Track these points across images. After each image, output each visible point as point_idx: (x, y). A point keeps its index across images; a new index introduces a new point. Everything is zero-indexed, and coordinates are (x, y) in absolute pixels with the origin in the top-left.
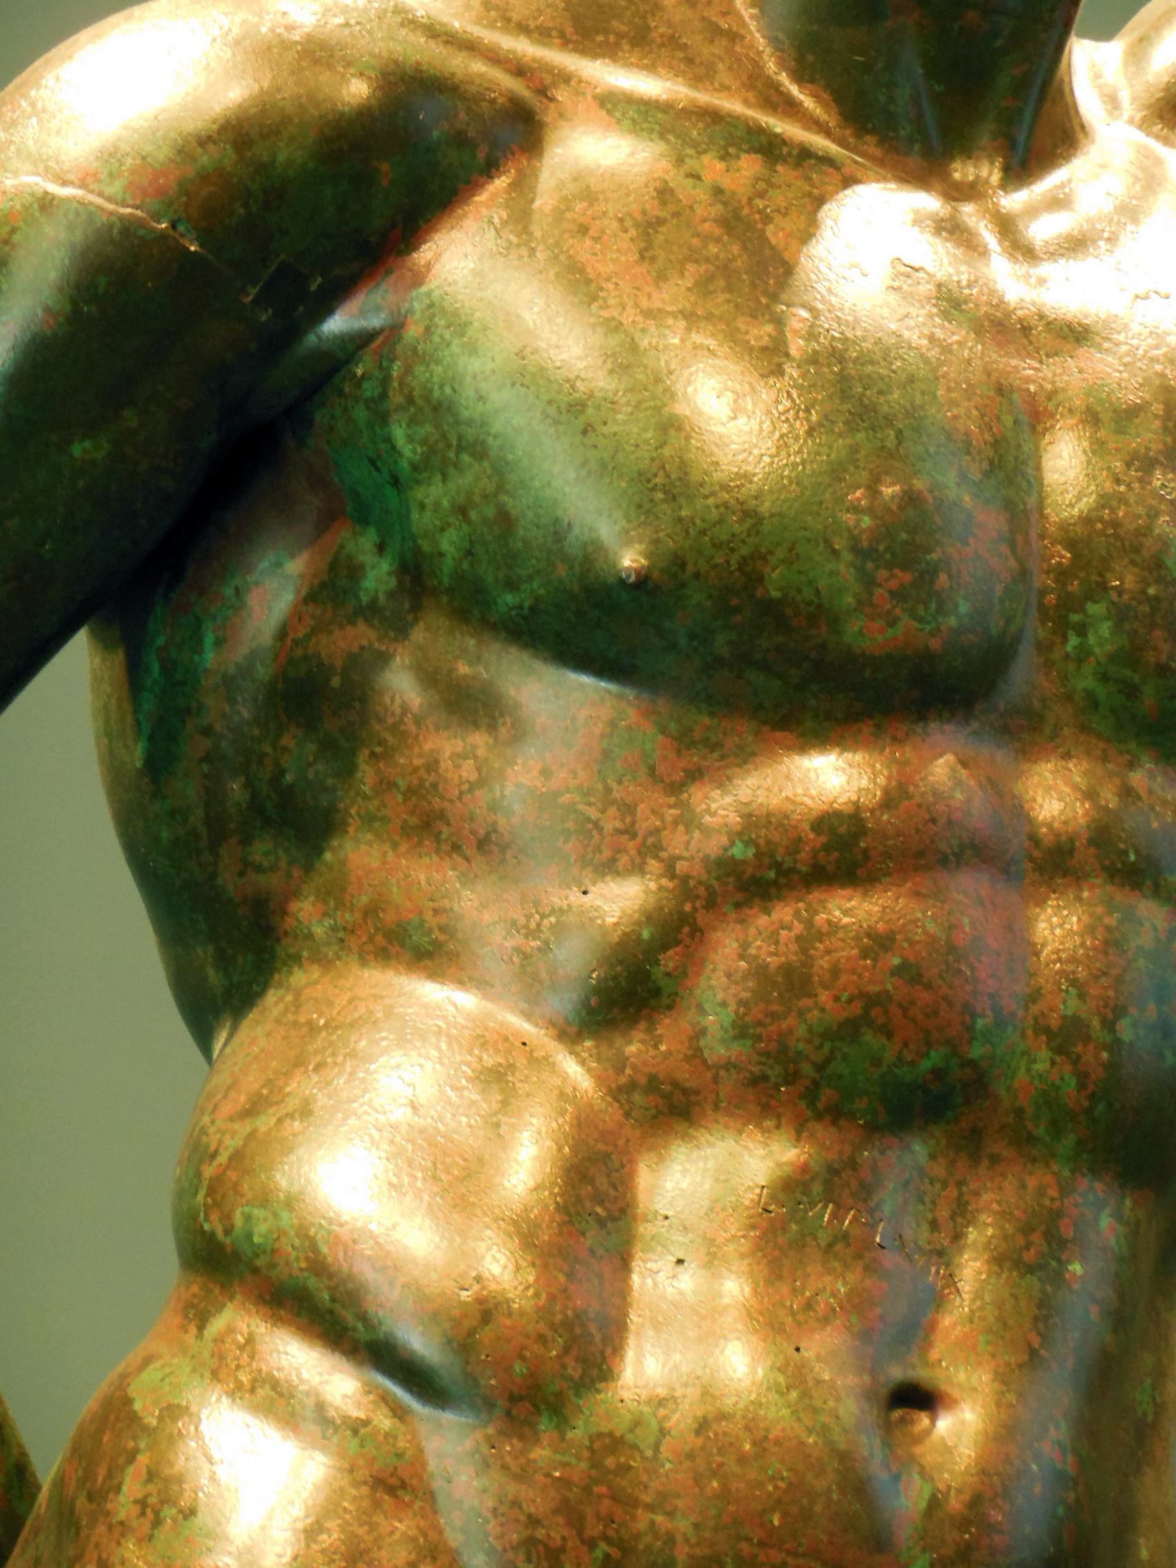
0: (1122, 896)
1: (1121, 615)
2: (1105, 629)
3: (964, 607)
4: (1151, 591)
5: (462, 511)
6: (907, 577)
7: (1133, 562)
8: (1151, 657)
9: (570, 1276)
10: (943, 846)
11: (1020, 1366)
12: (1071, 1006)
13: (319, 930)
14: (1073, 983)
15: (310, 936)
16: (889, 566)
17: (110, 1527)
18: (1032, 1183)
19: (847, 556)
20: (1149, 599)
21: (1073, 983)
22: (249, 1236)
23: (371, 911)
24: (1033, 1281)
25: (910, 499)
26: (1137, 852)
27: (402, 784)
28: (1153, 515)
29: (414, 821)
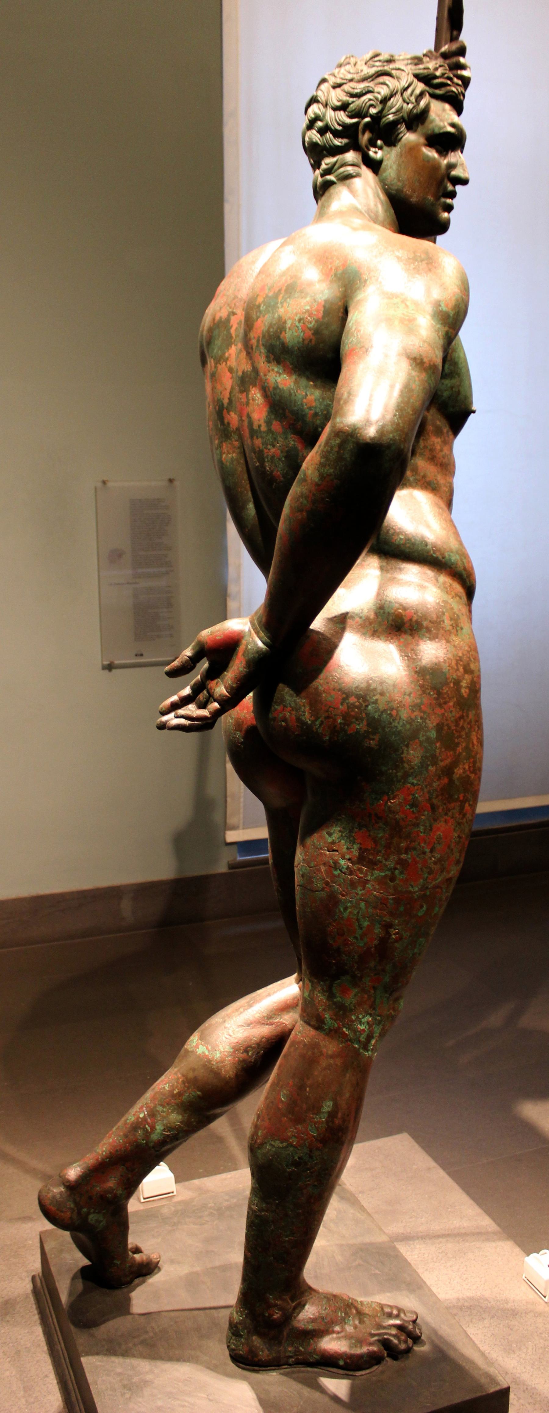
5: (452, 388)
13: (411, 479)
15: (409, 480)
17: (445, 631)
22: (450, 560)
23: (424, 477)
27: (429, 447)
29: (430, 457)
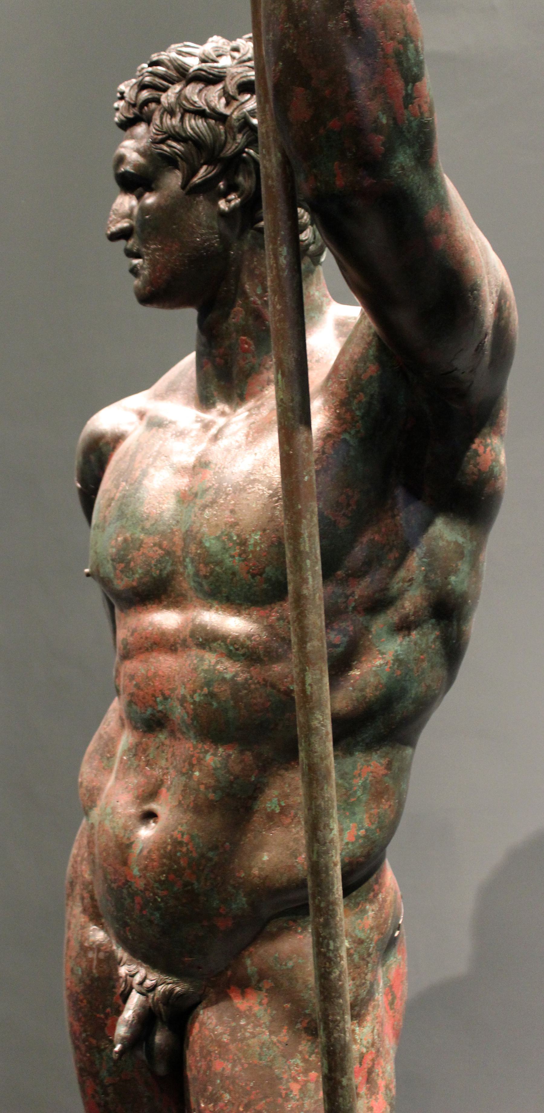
0: (201, 652)
1: (192, 561)
2: (190, 566)
3: (140, 571)
4: (199, 551)
6: (122, 565)
7: (194, 543)
8: (201, 573)
9: (96, 775)
10: (146, 645)
11: (176, 806)
12: (182, 691)
14: (184, 684)
16: (119, 563)
18: (187, 746)
19: (111, 562)
20: (200, 554)
21: (184, 684)
24: (184, 779)
25: (125, 540)
26: (202, 637)
28: (201, 526)
